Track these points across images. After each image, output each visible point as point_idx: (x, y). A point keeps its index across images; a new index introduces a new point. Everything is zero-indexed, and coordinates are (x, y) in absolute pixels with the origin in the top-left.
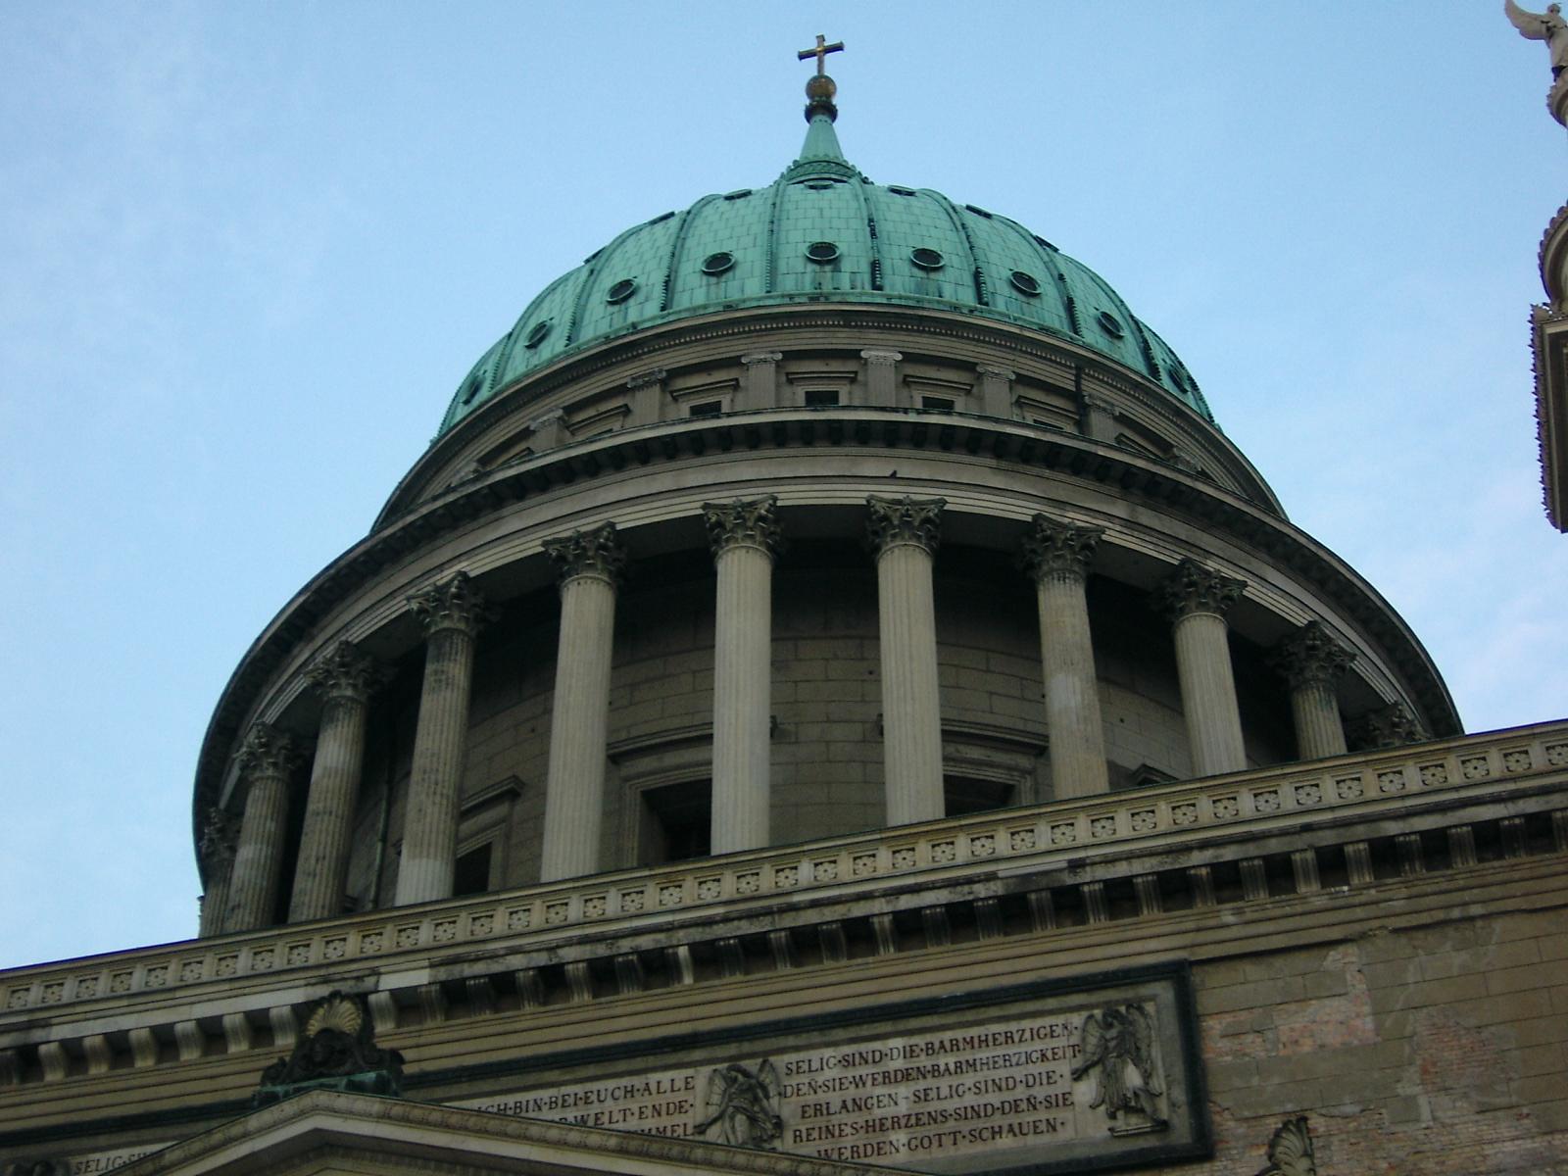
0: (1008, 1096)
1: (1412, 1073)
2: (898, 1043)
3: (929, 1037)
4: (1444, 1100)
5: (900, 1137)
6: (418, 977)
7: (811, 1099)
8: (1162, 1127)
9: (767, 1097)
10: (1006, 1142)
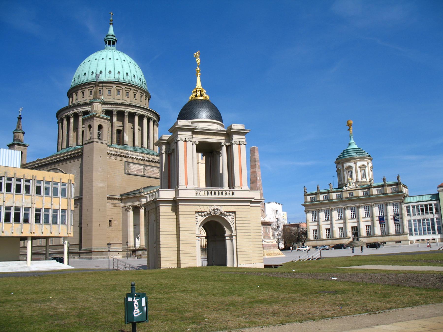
6: (148, 159)
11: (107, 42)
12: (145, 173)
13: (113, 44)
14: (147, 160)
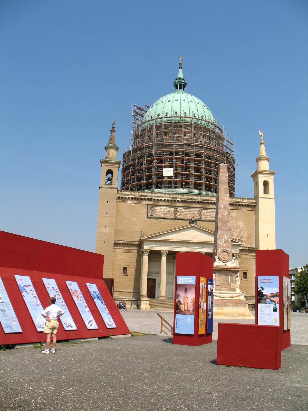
2: (209, 210)
5: (209, 217)
6: (179, 200)
11: (178, 85)
12: (177, 215)
13: (185, 86)
14: (178, 201)
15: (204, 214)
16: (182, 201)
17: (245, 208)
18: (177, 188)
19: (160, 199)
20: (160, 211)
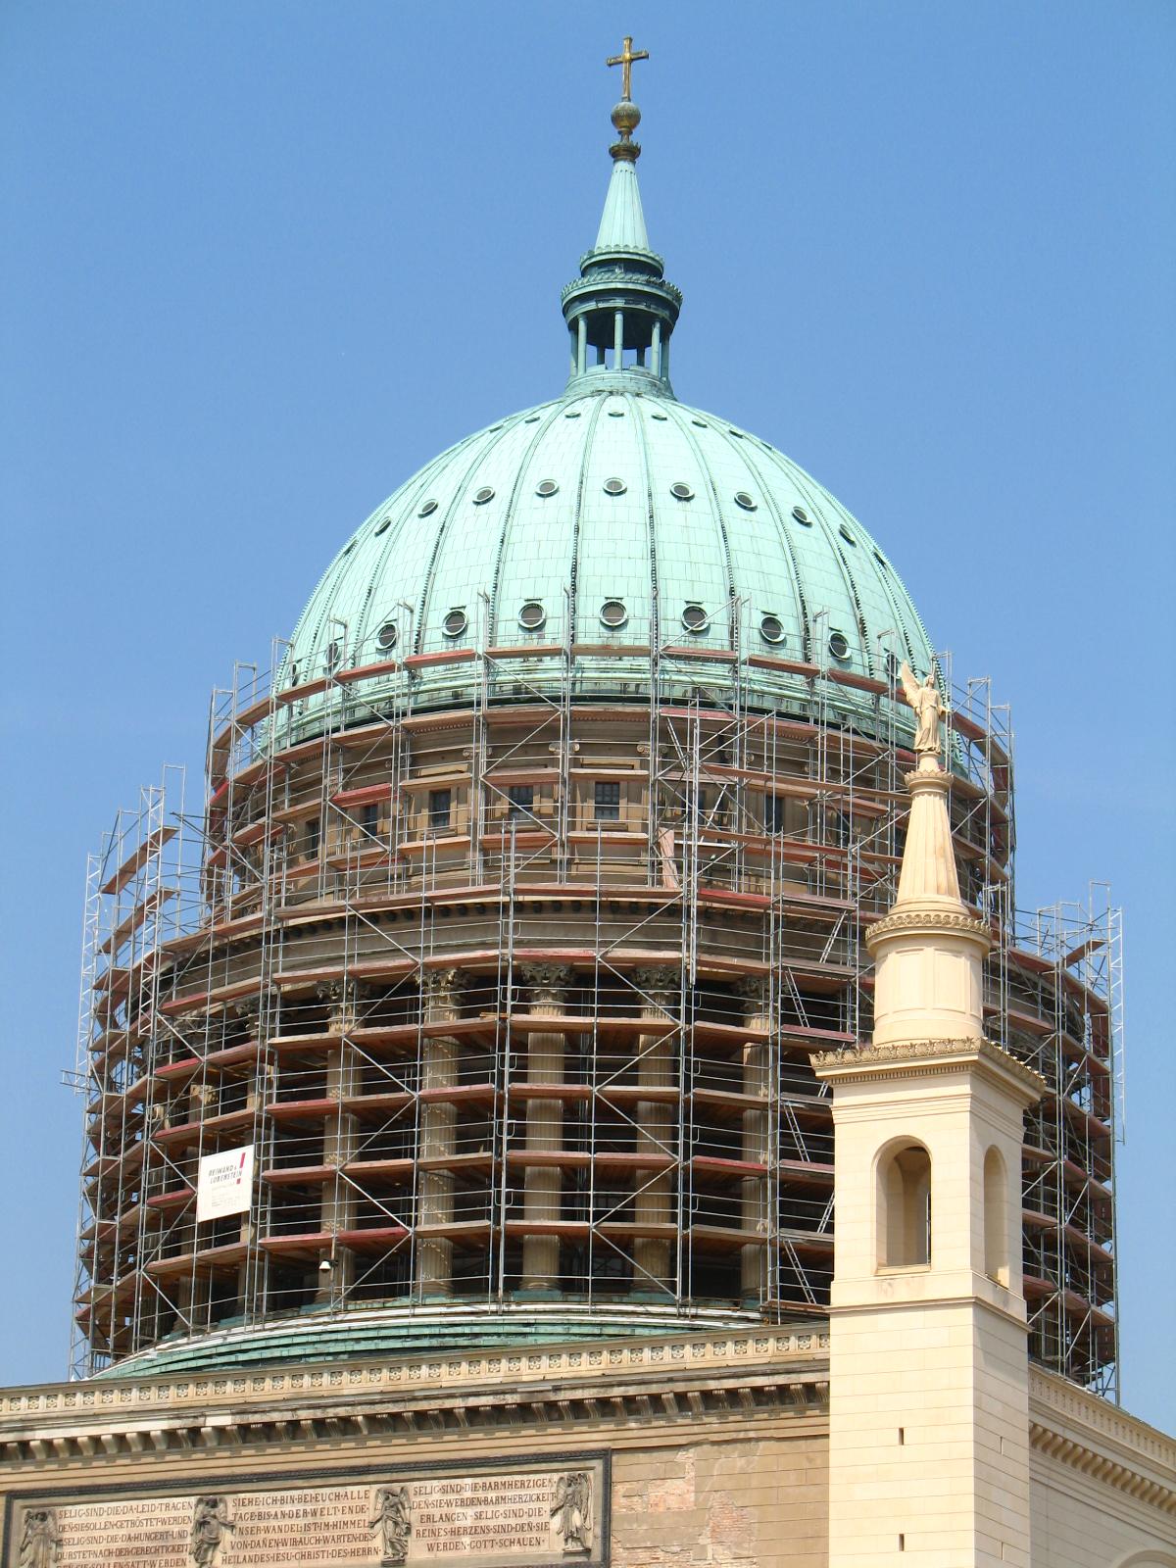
0: (520, 1521)
1: (707, 1531)
3: (484, 1479)
4: (720, 1548)
5: (466, 1540)
6: (225, 1421)
7: (425, 1511)
8: (587, 1551)
9: (404, 1508)
10: (516, 1549)
14: (220, 1431)
15: (429, 1518)
16: (244, 1430)
17: (762, 1422)
18: (304, 1309)
19: (82, 1433)
20: (96, 1534)
